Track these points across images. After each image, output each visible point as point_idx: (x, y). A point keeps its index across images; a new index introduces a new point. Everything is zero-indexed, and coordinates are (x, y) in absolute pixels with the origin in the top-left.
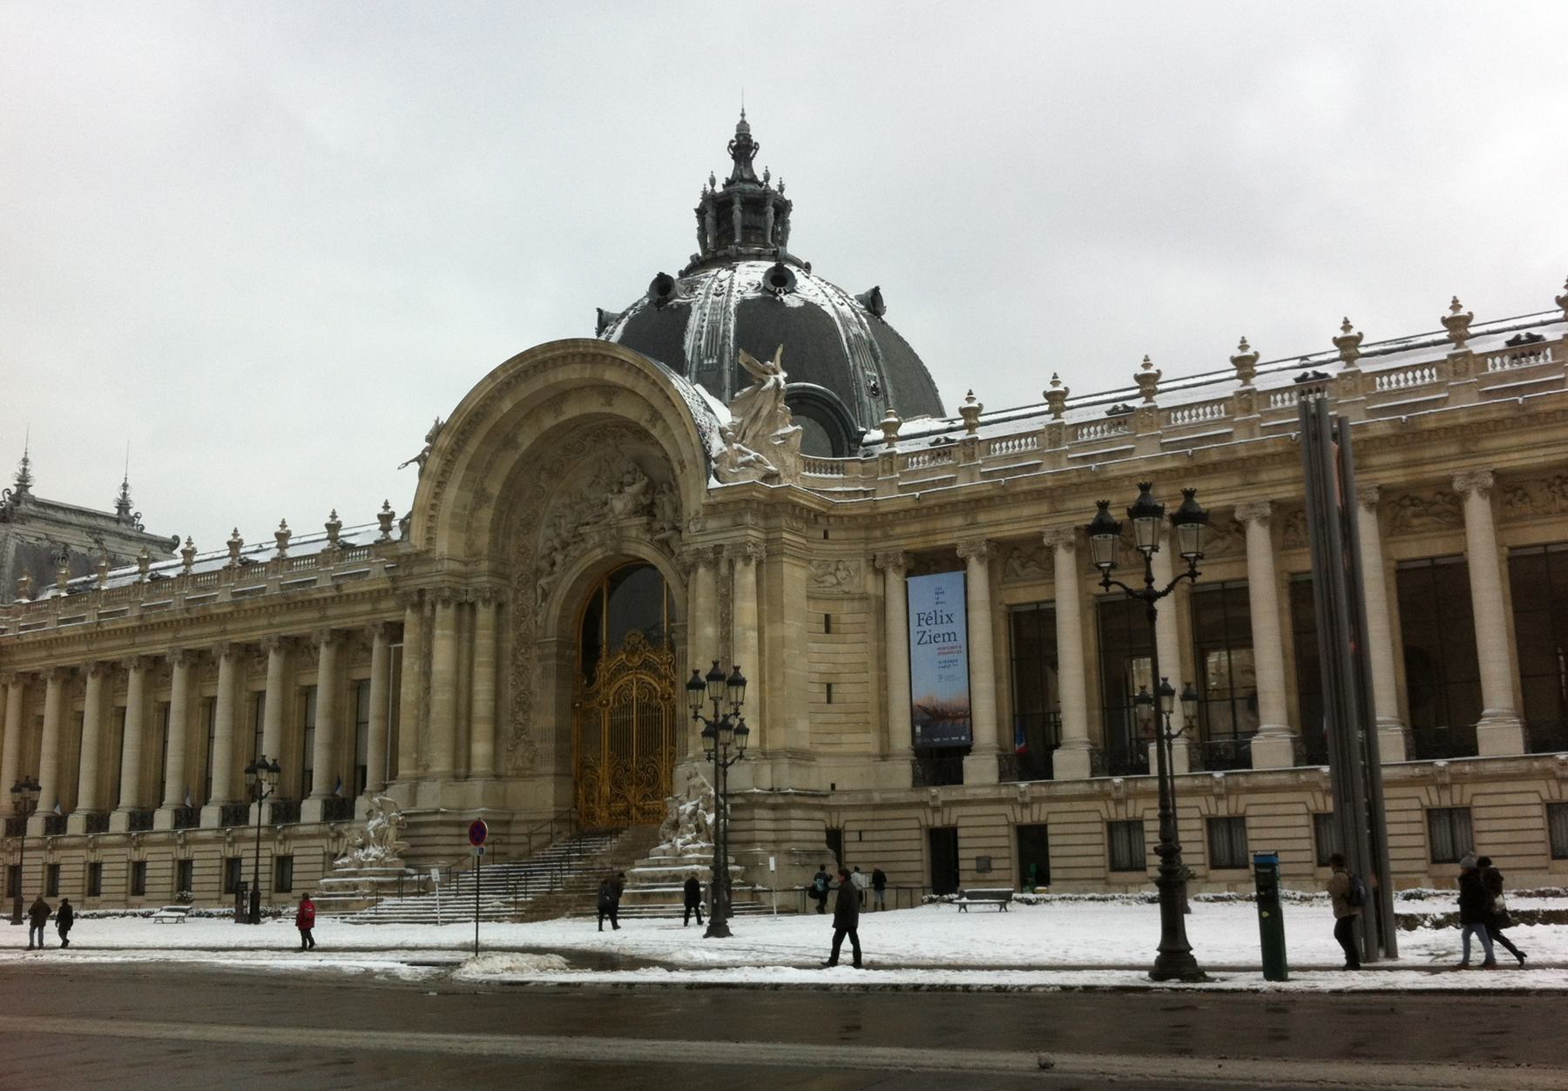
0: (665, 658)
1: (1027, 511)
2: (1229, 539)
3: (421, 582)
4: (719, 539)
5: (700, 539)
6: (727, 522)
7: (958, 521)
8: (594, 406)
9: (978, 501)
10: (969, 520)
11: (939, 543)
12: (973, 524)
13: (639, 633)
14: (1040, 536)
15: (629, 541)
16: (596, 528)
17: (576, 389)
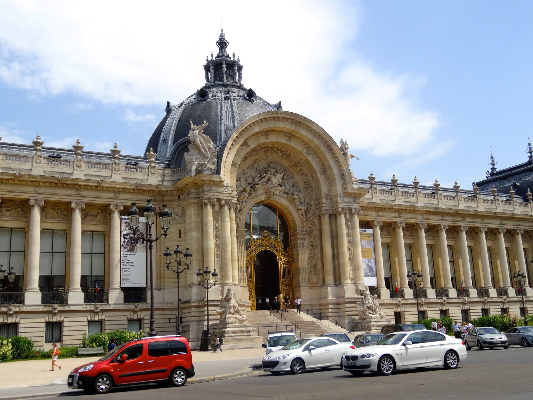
0: (279, 244)
1: (393, 214)
2: (430, 233)
3: (217, 196)
4: (350, 205)
5: (342, 204)
6: (352, 200)
7: (374, 213)
8: (283, 140)
9: (382, 208)
10: (377, 214)
11: (369, 219)
12: (378, 215)
13: (267, 232)
14: (70, 203)
15: (277, 195)
16: (263, 187)
17: (278, 131)
